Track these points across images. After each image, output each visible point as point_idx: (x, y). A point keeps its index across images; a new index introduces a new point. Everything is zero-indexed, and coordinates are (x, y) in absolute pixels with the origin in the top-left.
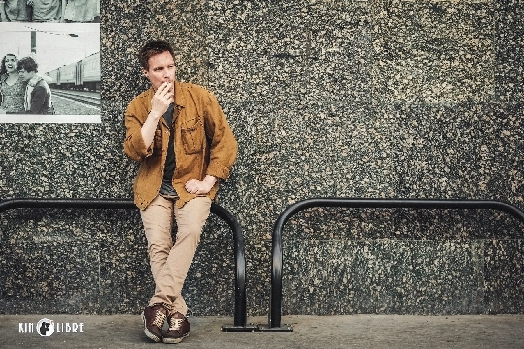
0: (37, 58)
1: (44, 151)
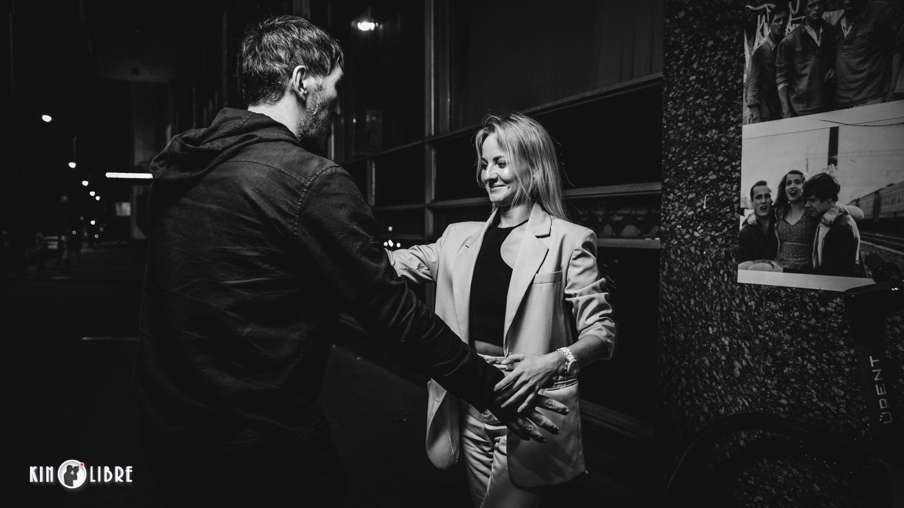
0: (839, 174)
1: (842, 343)
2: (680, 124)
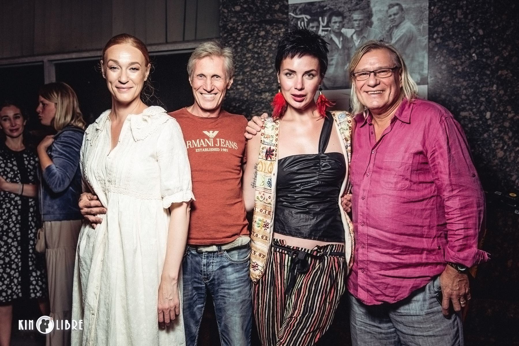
2: (239, 87)
